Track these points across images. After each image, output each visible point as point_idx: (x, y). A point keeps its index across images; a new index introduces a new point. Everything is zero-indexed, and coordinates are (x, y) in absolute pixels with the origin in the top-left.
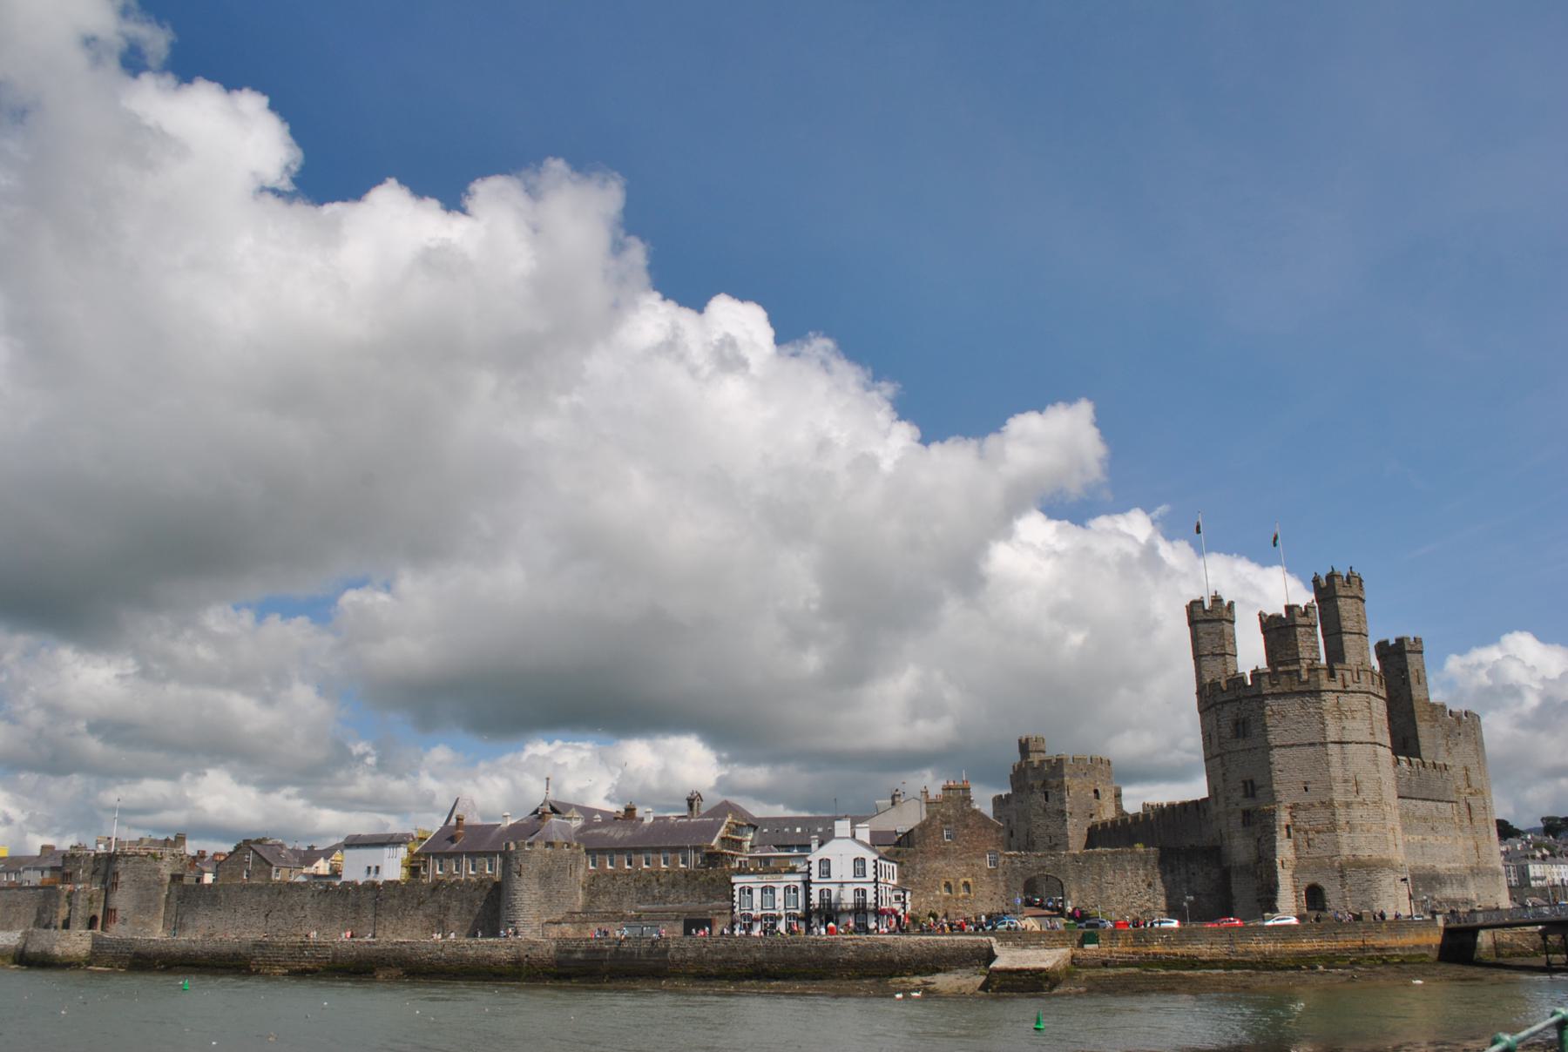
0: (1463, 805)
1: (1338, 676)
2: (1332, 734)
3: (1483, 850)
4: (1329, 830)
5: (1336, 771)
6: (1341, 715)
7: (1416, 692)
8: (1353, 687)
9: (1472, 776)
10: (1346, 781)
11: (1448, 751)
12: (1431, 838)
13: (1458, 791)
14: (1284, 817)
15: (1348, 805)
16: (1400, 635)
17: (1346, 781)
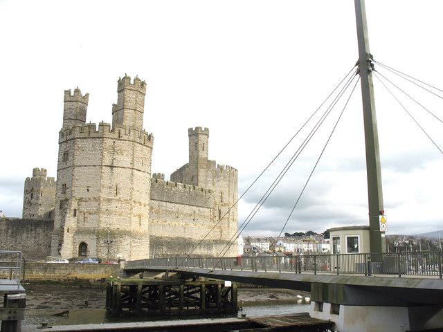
0: (217, 212)
1: (117, 131)
2: (107, 161)
3: (224, 232)
4: (96, 213)
5: (106, 181)
6: (113, 151)
7: (202, 154)
8: (124, 137)
9: (224, 197)
10: (110, 187)
11: (213, 184)
12: (192, 225)
13: (215, 203)
14: (74, 205)
15: (109, 200)
16: (197, 126)
17: (110, 187)
